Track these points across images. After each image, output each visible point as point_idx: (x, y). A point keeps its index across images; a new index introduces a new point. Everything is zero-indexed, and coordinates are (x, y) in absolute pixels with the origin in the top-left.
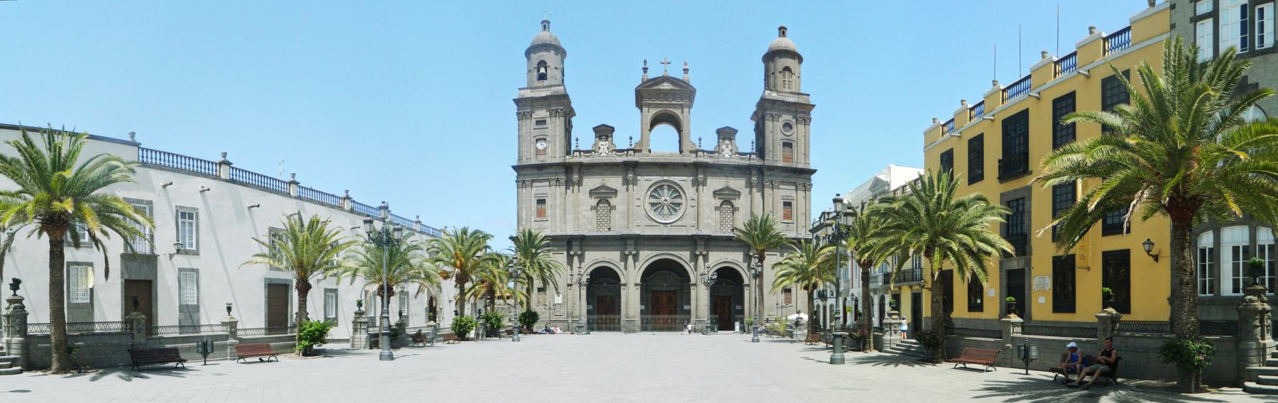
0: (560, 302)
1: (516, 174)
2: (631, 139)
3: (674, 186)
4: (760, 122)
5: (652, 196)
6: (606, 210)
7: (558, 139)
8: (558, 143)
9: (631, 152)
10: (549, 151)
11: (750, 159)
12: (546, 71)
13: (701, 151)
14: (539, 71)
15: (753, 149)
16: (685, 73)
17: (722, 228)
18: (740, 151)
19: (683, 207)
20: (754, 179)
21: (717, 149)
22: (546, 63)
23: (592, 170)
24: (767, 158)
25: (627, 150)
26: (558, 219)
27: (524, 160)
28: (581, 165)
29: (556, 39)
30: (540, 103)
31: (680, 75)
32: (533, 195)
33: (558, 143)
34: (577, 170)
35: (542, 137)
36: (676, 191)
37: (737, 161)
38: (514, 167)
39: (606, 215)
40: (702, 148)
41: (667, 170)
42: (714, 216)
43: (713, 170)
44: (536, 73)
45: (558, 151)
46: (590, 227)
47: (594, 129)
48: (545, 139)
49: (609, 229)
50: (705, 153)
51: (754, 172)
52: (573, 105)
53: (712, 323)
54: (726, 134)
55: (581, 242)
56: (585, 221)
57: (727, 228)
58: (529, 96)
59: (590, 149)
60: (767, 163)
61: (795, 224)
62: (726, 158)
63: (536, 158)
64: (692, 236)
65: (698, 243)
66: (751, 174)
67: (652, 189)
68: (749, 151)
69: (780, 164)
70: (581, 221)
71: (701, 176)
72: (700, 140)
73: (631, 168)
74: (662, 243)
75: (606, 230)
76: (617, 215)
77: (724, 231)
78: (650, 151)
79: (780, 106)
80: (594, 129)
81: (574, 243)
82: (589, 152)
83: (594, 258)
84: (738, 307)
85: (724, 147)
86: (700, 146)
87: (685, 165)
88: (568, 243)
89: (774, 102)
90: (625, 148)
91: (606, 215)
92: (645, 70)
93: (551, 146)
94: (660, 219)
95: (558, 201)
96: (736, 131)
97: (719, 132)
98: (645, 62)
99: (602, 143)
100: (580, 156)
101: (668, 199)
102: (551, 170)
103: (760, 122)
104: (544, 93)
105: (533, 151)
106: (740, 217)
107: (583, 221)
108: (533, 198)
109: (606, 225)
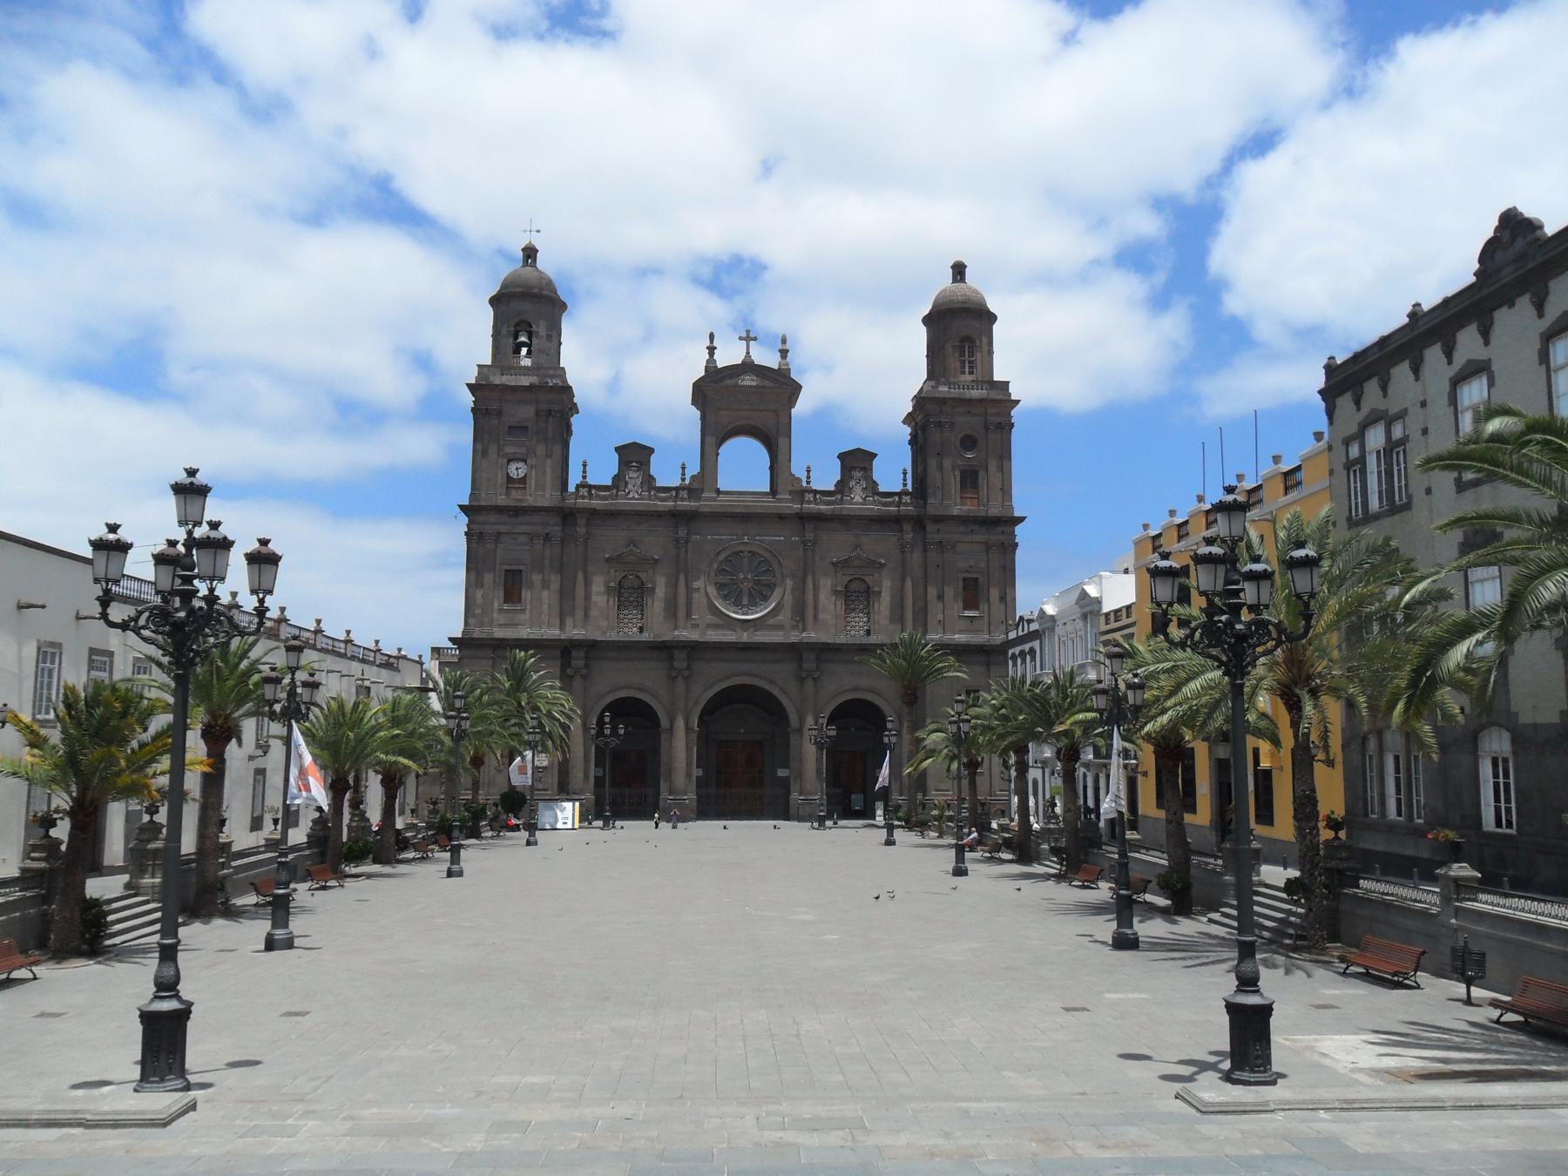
1: (465, 520)
2: (683, 468)
3: (762, 552)
5: (721, 571)
6: (635, 595)
8: (549, 470)
9: (684, 494)
10: (532, 483)
11: (899, 504)
14: (516, 337)
15: (905, 485)
17: (849, 628)
18: (882, 489)
20: (909, 537)
22: (531, 327)
24: (931, 501)
25: (677, 489)
26: (545, 607)
27: (483, 495)
28: (593, 513)
33: (549, 470)
36: (766, 561)
37: (873, 508)
38: (462, 508)
39: (635, 603)
40: (815, 486)
42: (833, 607)
44: (511, 340)
45: (548, 486)
46: (604, 624)
47: (617, 449)
48: (525, 461)
49: (641, 630)
51: (907, 527)
52: (575, 400)
53: (829, 803)
54: (857, 462)
59: (609, 483)
60: (931, 511)
61: (986, 617)
63: (508, 494)
66: (901, 531)
67: (721, 558)
68: (898, 488)
69: (955, 513)
71: (810, 536)
72: (808, 471)
77: (853, 632)
78: (718, 492)
80: (617, 449)
81: (574, 653)
82: (606, 488)
83: (615, 681)
85: (852, 483)
86: (808, 483)
87: (781, 517)
89: (942, 401)
90: (675, 486)
91: (635, 603)
92: (712, 350)
94: (734, 612)
96: (874, 455)
97: (842, 456)
98: (712, 337)
99: (632, 474)
100: (590, 493)
101: (749, 577)
102: (536, 518)
104: (525, 381)
105: (501, 479)
107: (594, 612)
108: (497, 567)
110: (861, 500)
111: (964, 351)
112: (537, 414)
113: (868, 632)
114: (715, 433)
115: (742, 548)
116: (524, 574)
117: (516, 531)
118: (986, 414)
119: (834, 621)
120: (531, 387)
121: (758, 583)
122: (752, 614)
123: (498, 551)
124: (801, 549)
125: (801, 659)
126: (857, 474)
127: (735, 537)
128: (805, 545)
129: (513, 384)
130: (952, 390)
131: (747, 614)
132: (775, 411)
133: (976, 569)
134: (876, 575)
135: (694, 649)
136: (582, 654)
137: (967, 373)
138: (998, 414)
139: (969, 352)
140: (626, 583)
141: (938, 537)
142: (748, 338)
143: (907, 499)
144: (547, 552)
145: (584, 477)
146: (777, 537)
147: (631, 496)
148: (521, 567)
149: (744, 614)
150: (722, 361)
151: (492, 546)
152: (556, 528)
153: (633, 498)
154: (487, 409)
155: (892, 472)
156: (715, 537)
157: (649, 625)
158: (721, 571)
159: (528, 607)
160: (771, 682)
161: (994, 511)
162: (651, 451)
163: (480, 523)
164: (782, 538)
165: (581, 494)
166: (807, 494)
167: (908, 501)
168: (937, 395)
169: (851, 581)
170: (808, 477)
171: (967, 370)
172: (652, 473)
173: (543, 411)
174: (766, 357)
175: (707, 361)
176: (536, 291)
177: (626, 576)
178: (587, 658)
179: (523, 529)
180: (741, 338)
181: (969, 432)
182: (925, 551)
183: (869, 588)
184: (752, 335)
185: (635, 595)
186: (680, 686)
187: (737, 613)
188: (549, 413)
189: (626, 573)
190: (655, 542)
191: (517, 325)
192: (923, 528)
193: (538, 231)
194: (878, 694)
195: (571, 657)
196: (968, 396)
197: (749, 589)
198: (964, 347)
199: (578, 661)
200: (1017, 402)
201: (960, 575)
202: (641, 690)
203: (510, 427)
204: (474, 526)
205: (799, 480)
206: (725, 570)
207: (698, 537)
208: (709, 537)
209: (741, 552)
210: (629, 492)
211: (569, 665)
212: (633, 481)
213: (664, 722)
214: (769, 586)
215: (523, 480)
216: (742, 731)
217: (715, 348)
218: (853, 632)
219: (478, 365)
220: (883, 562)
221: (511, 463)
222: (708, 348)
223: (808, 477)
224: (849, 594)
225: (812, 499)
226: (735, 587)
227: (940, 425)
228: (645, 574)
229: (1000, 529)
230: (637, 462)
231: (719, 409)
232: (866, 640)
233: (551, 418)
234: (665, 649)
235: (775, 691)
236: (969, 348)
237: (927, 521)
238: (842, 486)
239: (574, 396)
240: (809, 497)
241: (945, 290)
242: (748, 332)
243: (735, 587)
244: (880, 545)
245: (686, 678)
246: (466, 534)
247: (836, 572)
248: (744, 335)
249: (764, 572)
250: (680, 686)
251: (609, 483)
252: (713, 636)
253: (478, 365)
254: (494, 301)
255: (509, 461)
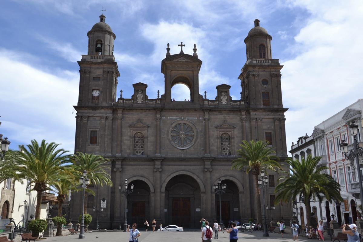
0: (105, 206)
1: (76, 112)
2: (158, 92)
3: (189, 124)
4: (246, 81)
7: (108, 90)
9: (159, 102)
12: (102, 45)
13: (206, 100)
16: (194, 52)
17: (223, 152)
18: (233, 99)
19: (195, 137)
20: (244, 117)
21: (217, 99)
22: (102, 42)
23: (131, 112)
24: (252, 103)
25: (156, 100)
29: (109, 28)
30: (97, 66)
31: (191, 53)
32: (88, 127)
34: (121, 112)
35: (97, 88)
38: (75, 107)
39: (140, 144)
41: (183, 113)
43: (215, 113)
44: (95, 47)
46: (128, 151)
47: (134, 86)
48: (99, 90)
49: (143, 154)
50: (209, 102)
51: (243, 113)
55: (122, 162)
56: (126, 147)
57: (226, 152)
58: (89, 61)
59: (131, 98)
62: (224, 105)
64: (202, 158)
65: (206, 163)
66: (241, 115)
67: (173, 125)
68: (239, 99)
70: (123, 147)
71: (207, 116)
73: (158, 112)
74: (180, 163)
75: (140, 154)
76: (148, 144)
77: (224, 154)
79: (259, 69)
81: (117, 163)
84: (236, 210)
85: (222, 97)
86: (205, 97)
88: (112, 162)
89: (254, 66)
92: (168, 49)
93: (103, 95)
94: (178, 146)
95: (107, 132)
97: (218, 88)
98: (168, 45)
100: (123, 102)
101: (184, 133)
102: (102, 111)
103: (246, 81)
104: (99, 61)
106: (235, 144)
107: (124, 147)
108: (88, 130)
109: (140, 150)
110: (225, 103)
111: (261, 50)
112: (104, 72)
113: (230, 154)
114: (169, 84)
115: (181, 122)
116: (98, 132)
117: (95, 116)
118: (271, 71)
119: (217, 150)
120: (101, 63)
121: (187, 135)
122: (185, 147)
123: (88, 124)
124: (204, 122)
125: (205, 165)
126: (224, 94)
127: (178, 118)
128: (205, 120)
129: (95, 61)
130: (258, 63)
131: (183, 147)
132: (192, 71)
133: (270, 129)
134: (233, 132)
135: (163, 160)
136: (120, 163)
137: (262, 57)
138: (275, 71)
139: (263, 50)
140: (137, 136)
141: (255, 117)
142: (182, 45)
143: (243, 103)
144: (107, 124)
145: (121, 96)
146: (193, 118)
147: (139, 102)
148: (97, 130)
149: (182, 147)
150: (172, 53)
151: (86, 121)
152: (110, 115)
153: (140, 103)
154: (85, 71)
155: (236, 95)
156: (171, 118)
157: (146, 151)
158: (173, 131)
159: (100, 145)
160: (193, 173)
161: (276, 107)
162: (146, 86)
163: (81, 113)
164: (196, 118)
165: (120, 102)
166: (205, 101)
167: (243, 104)
168: (252, 64)
169: (223, 134)
170: (205, 95)
171: (262, 56)
172: (147, 94)
173: (106, 71)
174: (188, 51)
175: (167, 53)
176: (104, 29)
177: (137, 133)
178: (122, 165)
179: (98, 115)
180: (179, 45)
181: (265, 78)
182: (250, 122)
183: (230, 137)
184: (183, 44)
185: (140, 140)
186: (158, 174)
187: (180, 147)
188: (108, 72)
189: (137, 132)
190: (148, 118)
191: (97, 41)
192: (249, 113)
193: (105, 10)
194: (235, 177)
195: (115, 164)
196: (264, 65)
197: (184, 138)
198: (261, 48)
199: (118, 164)
200: (282, 66)
201: (264, 131)
202: (143, 177)
203: (94, 78)
204: (79, 114)
205: (202, 96)
206: (174, 130)
207: (164, 118)
208: (168, 118)
209: (181, 123)
210: (138, 101)
211: (115, 167)
212: (139, 97)
213: (152, 190)
214: (191, 136)
215: (98, 97)
216: (182, 193)
217: (170, 49)
218: (224, 154)
219: (82, 55)
220: (235, 126)
221: (94, 91)
222: (167, 49)
223: (205, 95)
224: (222, 139)
225: (207, 103)
226: (178, 137)
227: (254, 75)
228: (144, 132)
229: (279, 113)
230: (141, 90)
231: (172, 70)
232: (229, 157)
233: (109, 74)
234: (152, 160)
235: (194, 177)
236: (263, 48)
237: (251, 111)
238: (218, 98)
239: (118, 68)
240: (206, 102)
241: (252, 29)
242: (182, 43)
243: (178, 137)
244: (233, 119)
245: (160, 172)
246: (76, 117)
247: (217, 131)
248: (180, 44)
249: (189, 131)
250: (158, 174)
251: (131, 98)
252: (170, 156)
253: (82, 55)
254: (89, 34)
255: (93, 90)
